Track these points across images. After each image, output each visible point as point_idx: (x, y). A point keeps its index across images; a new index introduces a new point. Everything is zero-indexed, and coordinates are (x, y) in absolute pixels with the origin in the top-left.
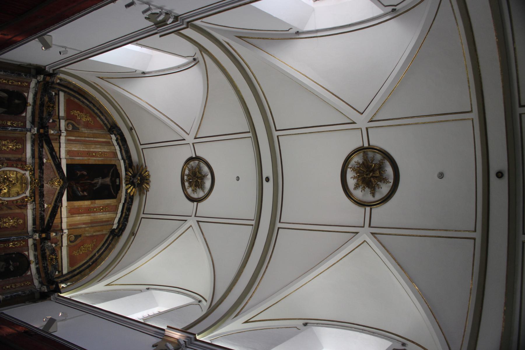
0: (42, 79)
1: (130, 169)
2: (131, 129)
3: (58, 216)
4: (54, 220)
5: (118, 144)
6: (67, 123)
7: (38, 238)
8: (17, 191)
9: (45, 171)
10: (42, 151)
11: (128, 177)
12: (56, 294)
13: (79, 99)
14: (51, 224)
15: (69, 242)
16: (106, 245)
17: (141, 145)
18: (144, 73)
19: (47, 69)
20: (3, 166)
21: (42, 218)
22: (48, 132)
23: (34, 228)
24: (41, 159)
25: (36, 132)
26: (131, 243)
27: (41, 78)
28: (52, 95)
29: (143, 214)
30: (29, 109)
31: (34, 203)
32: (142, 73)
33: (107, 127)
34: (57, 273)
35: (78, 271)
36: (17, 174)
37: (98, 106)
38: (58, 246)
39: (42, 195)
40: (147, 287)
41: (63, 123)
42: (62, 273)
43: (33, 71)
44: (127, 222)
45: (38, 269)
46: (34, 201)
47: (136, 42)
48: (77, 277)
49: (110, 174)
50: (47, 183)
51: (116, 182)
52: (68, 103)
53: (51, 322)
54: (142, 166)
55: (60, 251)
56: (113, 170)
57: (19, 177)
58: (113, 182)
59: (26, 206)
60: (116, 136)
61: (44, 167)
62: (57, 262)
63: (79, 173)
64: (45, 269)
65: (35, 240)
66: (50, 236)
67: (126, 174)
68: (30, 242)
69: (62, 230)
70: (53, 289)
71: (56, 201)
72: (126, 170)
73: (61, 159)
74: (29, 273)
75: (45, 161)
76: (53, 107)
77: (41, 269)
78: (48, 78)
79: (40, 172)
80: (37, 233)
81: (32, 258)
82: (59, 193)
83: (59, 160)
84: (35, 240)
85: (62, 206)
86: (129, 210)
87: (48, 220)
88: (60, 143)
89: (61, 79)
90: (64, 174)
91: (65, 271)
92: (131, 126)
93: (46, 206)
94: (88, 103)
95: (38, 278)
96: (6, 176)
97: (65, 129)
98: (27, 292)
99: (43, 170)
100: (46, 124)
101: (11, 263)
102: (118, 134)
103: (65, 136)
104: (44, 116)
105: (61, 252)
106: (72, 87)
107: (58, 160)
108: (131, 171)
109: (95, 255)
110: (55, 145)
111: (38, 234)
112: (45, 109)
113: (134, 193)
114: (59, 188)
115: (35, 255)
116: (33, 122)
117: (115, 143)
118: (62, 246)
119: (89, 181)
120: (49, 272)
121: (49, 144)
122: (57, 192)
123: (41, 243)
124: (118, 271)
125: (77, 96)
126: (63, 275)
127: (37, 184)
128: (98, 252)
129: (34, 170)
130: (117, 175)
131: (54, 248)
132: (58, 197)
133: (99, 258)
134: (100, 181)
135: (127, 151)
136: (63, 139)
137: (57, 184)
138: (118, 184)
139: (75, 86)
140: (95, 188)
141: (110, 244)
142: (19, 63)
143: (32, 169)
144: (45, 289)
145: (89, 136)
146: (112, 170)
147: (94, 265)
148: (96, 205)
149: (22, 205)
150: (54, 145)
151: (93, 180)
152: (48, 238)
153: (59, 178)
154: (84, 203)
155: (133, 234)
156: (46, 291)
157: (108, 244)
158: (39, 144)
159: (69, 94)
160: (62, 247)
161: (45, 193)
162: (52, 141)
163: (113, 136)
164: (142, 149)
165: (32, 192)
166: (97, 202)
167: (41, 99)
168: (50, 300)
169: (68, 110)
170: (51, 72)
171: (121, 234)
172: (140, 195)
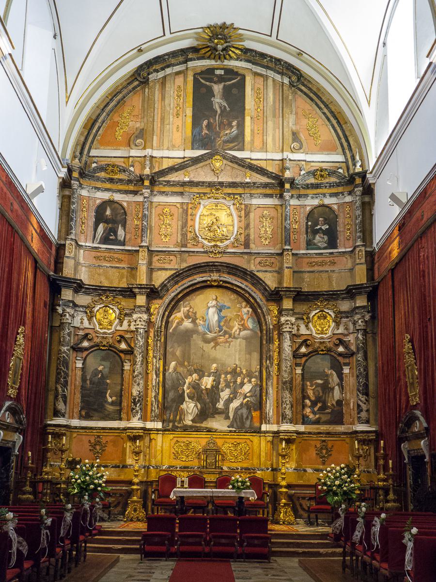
0: (78, 183)
1: (201, 53)
2: (140, 51)
3: (263, 164)
4: (267, 171)
5: (163, 69)
6: (133, 146)
7: (290, 194)
8: (226, 216)
9: (201, 180)
10: (174, 181)
11: (213, 56)
12: (368, 176)
13: (99, 128)
14: (274, 175)
15: (302, 151)
16: (312, 95)
17: (164, 35)
18: (55, 37)
19: (63, 176)
20: (193, 231)
21: (266, 186)
22: (148, 176)
23: (276, 197)
24: (183, 184)
25: (149, 191)
26: (314, 59)
27: (75, 184)
28: (96, 167)
29: (271, 36)
30: (118, 197)
31: (243, 195)
32: (55, 39)
33: (138, 86)
34: (340, 171)
35: (343, 140)
36: (203, 215)
37: (108, 100)
38: (304, 167)
39: (233, 185)
40: (382, 45)
41: (134, 153)
42: (342, 162)
43: (67, 192)
44: (282, 60)
45: (332, 195)
46: (240, 195)
47: (20, 71)
48: (352, 143)
49: (208, 83)
50: (218, 177)
51: (221, 75)
52: (105, 143)
53: (393, 198)
54: (196, 33)
55: (312, 164)
56: (201, 78)
57: (208, 213)
58: (221, 79)
59: (246, 206)
60: (152, 73)
61: (196, 180)
62: (326, 169)
63: (205, 131)
64: (333, 186)
65: (292, 196)
66: (289, 179)
67: (209, 58)
68: (294, 202)
69: (282, 160)
70: (361, 179)
71: (243, 166)
72: (202, 58)
73: (184, 158)
74: (336, 207)
75: (187, 179)
76: (113, 166)
77: (334, 190)
78: (75, 175)
79: (202, 186)
80: (283, 194)
81: (316, 202)
82: (231, 162)
83: (186, 159)
84: (292, 196)
85: (251, 159)
86: (263, 55)
87: (268, 177)
88: (162, 158)
89: (74, 157)
90: (205, 154)
91: (341, 158)
92: (135, 51)
93: (248, 180)
94: (105, 114)
95: (343, 197)
96: (207, 229)
97: (141, 149)
98: (359, 212)
99: (200, 182)
100: (137, 175)
101: (319, 227)
102: (149, 68)
103: (152, 149)
104: (126, 178)
105: (313, 162)
106: (83, 139)
107: (187, 161)
108: (203, 51)
109: (324, 114)
110: (166, 165)
111: (285, 194)
112: (116, 177)
113: (237, 48)
114: (225, 162)
115: (312, 198)
116: (135, 193)
117: (161, 75)
118: (305, 161)
119: (217, 117)
120: (338, 181)
121: (163, 173)
122: (230, 164)
123: (298, 188)
124: (351, 84)
125: (94, 131)
126: (346, 162)
127: (218, 189)
128: (320, 108)
129: (198, 193)
130: (209, 72)
131: (307, 173)
132: (237, 163)
133: (329, 108)
134: (218, 101)
135: (174, 54)
136: (156, 153)
137: (218, 164)
138: (222, 72)
139: (82, 134)
140: (228, 109)
141: (310, 89)
142: (58, 210)
143: (198, 196)
144: (359, 190)
145: (152, 114)
146: (203, 81)
147: (338, 116)
148: (253, 109)
149: (245, 210)
150: (165, 166)
151: (217, 112)
152: (292, 182)
153: (211, 160)
154: (248, 126)
155: (300, 54)
156: (361, 189)
157: (311, 92)
158: (165, 186)
159: (92, 142)
160: (307, 160)
161: (230, 180)
162: (161, 169)
163: (152, 77)
164: (171, 33)
165: (228, 196)
166: (247, 106)
167: (103, 182)
168: (374, 184)
169: (115, 144)
170: (65, 170)
171: (298, 70)
172: (242, 40)
